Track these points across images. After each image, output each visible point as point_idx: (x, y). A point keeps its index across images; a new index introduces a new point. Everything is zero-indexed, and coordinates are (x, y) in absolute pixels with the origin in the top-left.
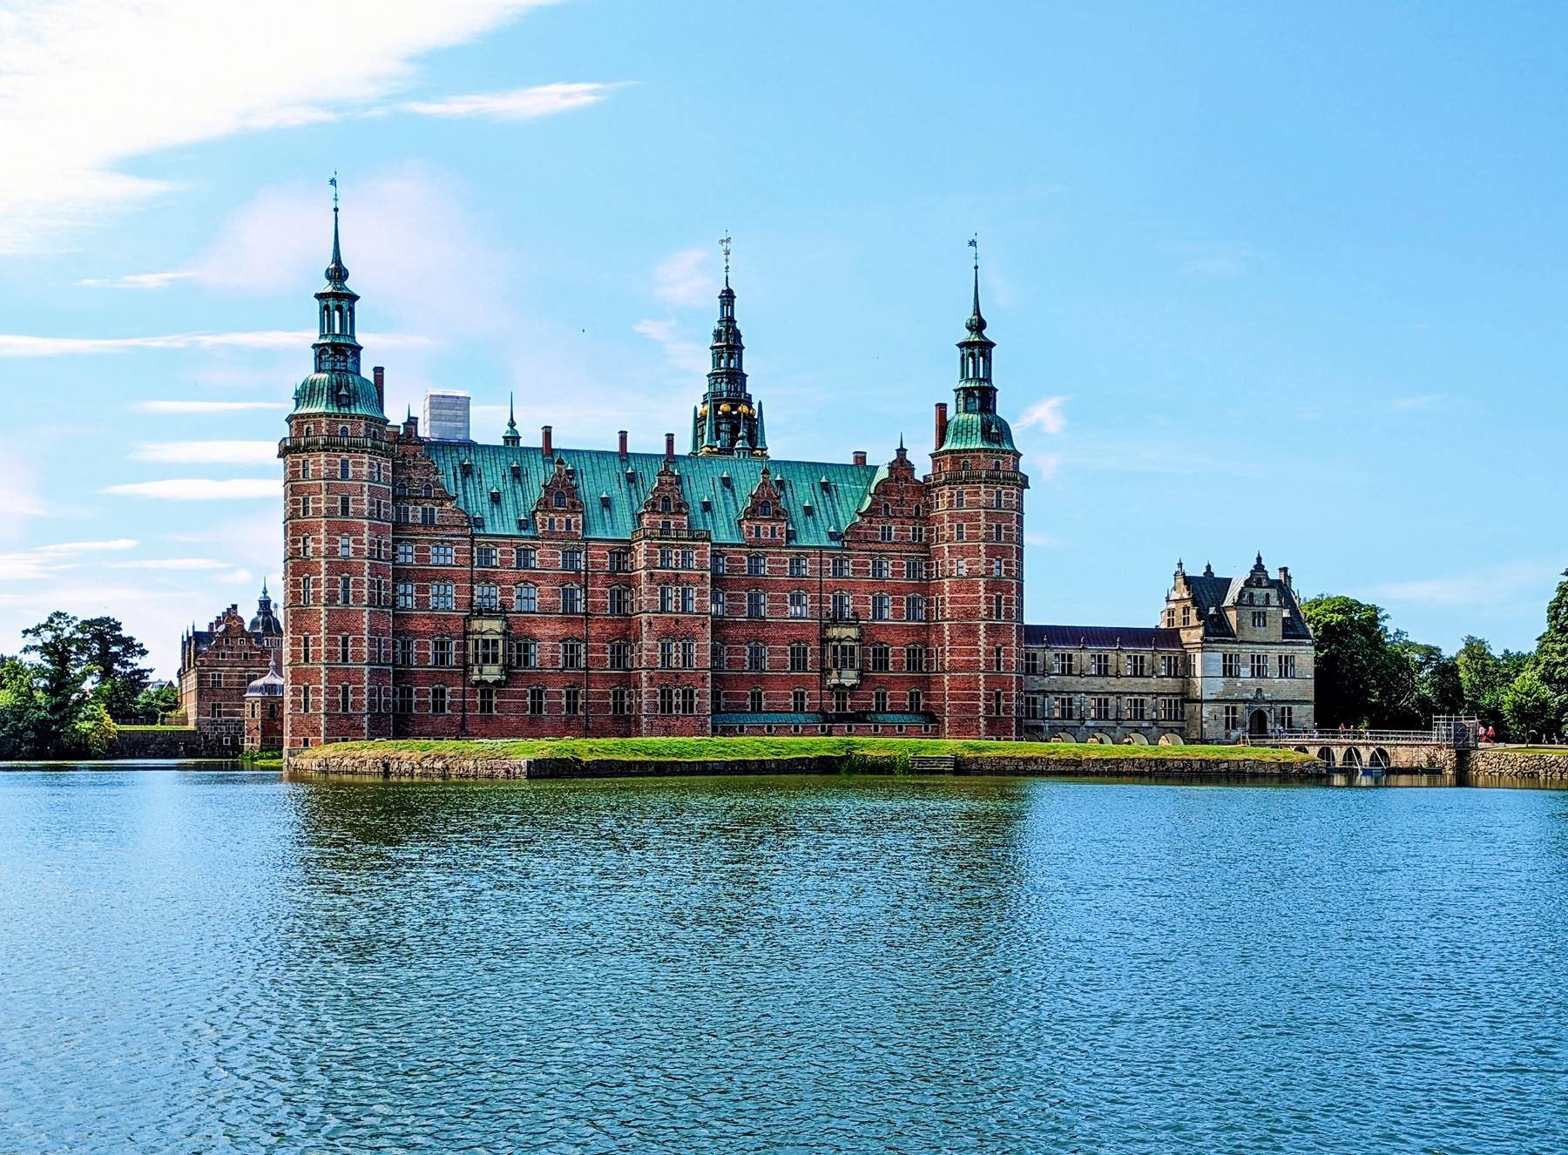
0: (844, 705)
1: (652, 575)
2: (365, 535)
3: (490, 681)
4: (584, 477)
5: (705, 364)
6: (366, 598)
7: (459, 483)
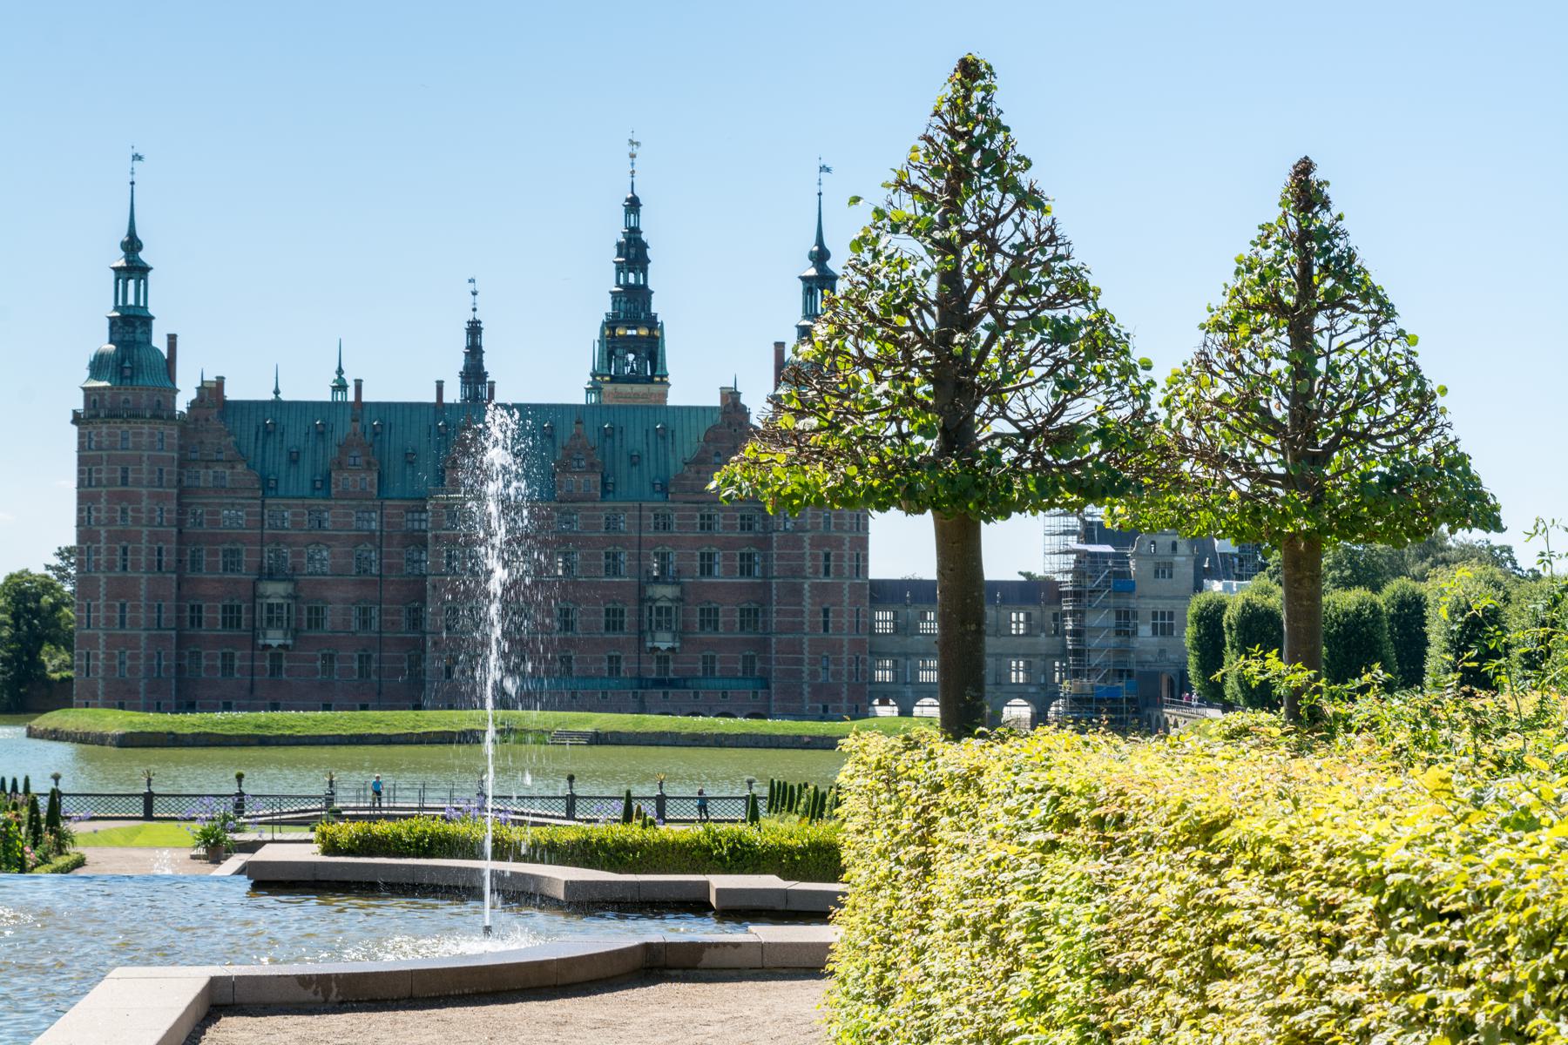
0: (667, 669)
2: (144, 504)
6: (143, 565)
7: (260, 443)
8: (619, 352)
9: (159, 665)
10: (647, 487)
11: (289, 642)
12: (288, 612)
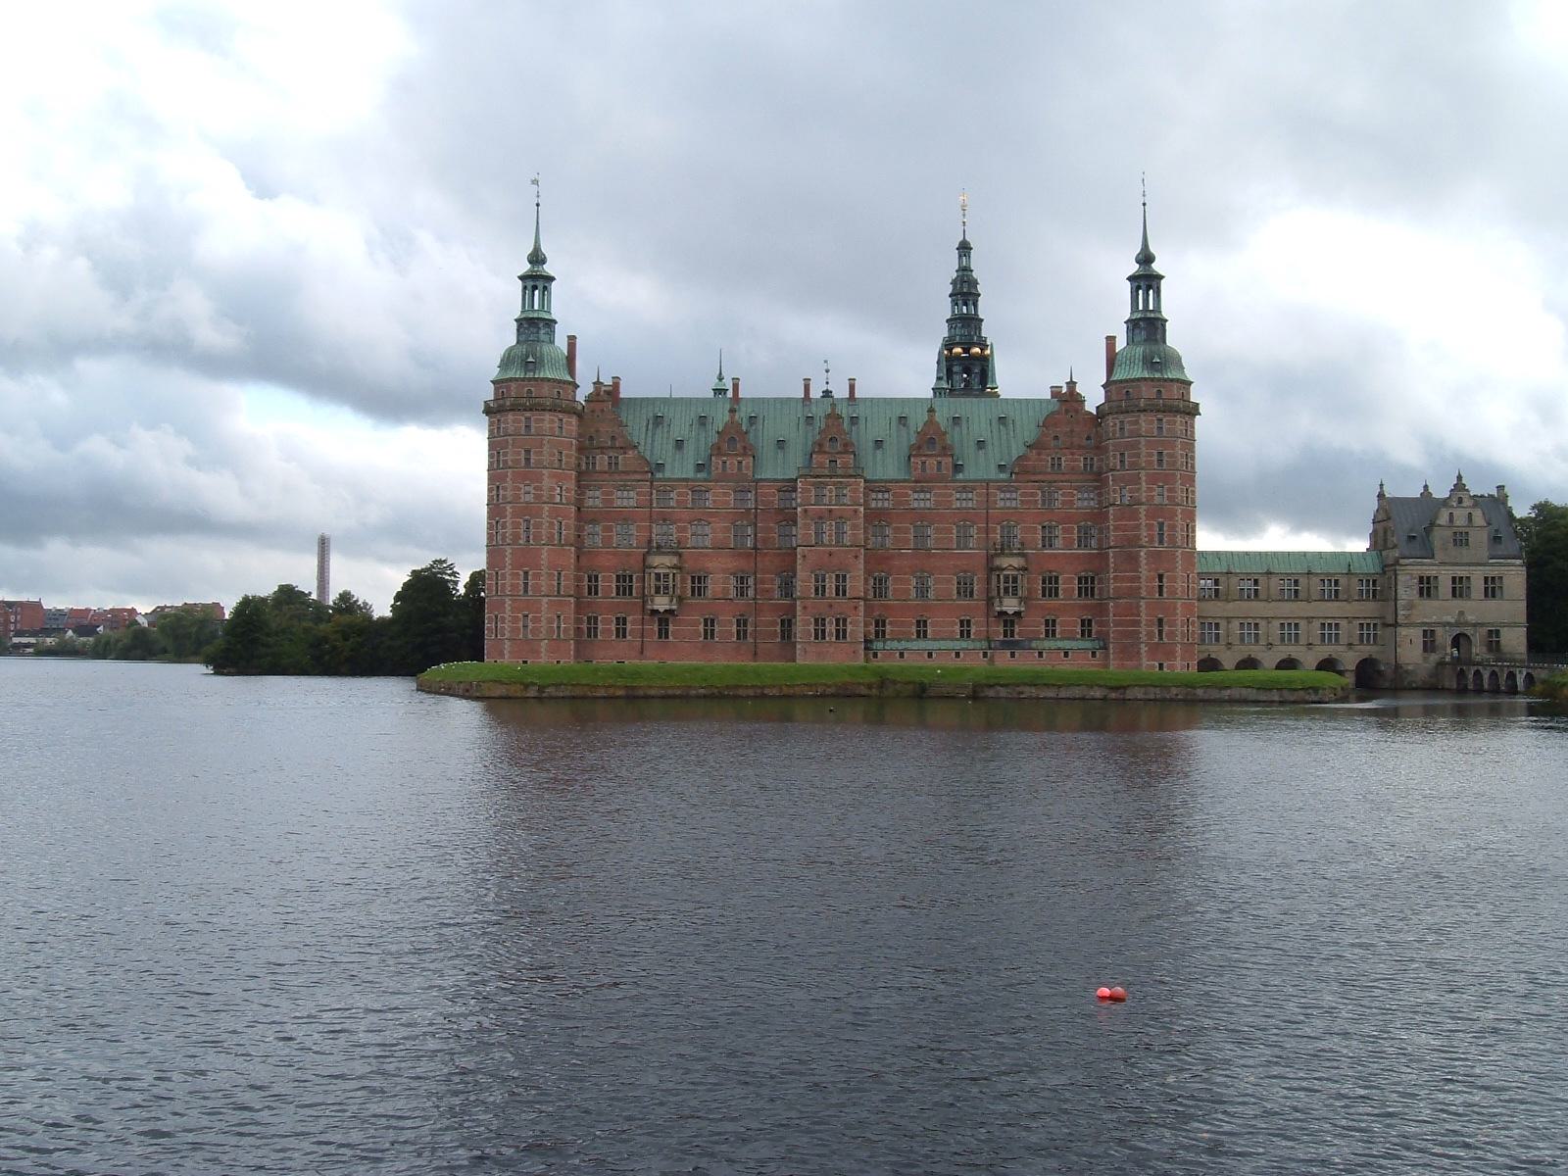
0: (1012, 632)
1: (806, 511)
3: (662, 610)
4: (766, 422)
8: (956, 369)
9: (559, 627)
10: (993, 468)
11: (674, 607)
12: (674, 580)
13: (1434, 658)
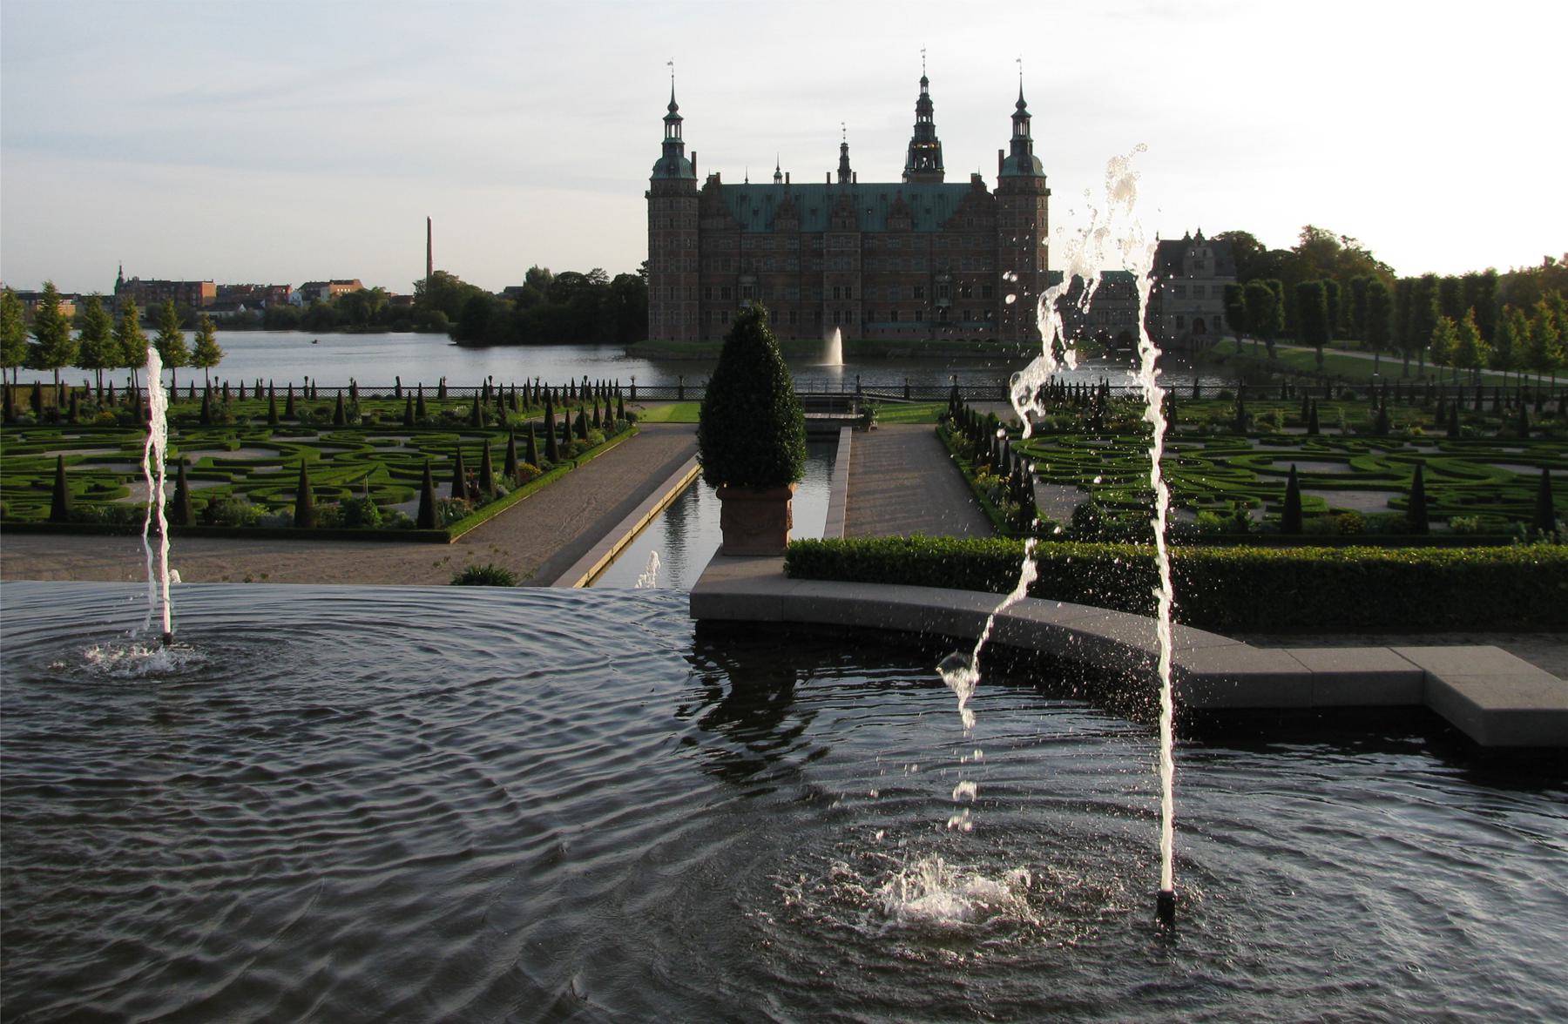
1: (828, 252)
5: (911, 118)
13: (1183, 331)
